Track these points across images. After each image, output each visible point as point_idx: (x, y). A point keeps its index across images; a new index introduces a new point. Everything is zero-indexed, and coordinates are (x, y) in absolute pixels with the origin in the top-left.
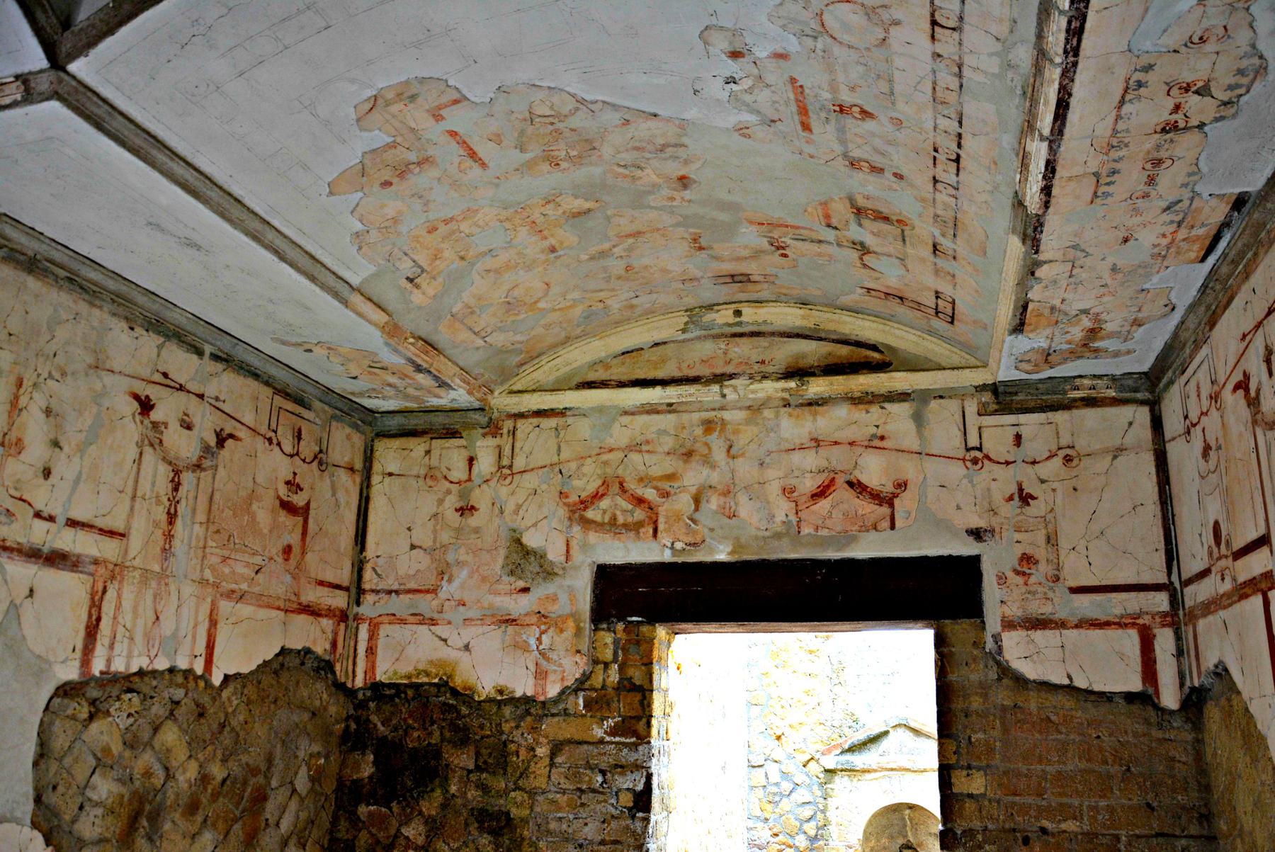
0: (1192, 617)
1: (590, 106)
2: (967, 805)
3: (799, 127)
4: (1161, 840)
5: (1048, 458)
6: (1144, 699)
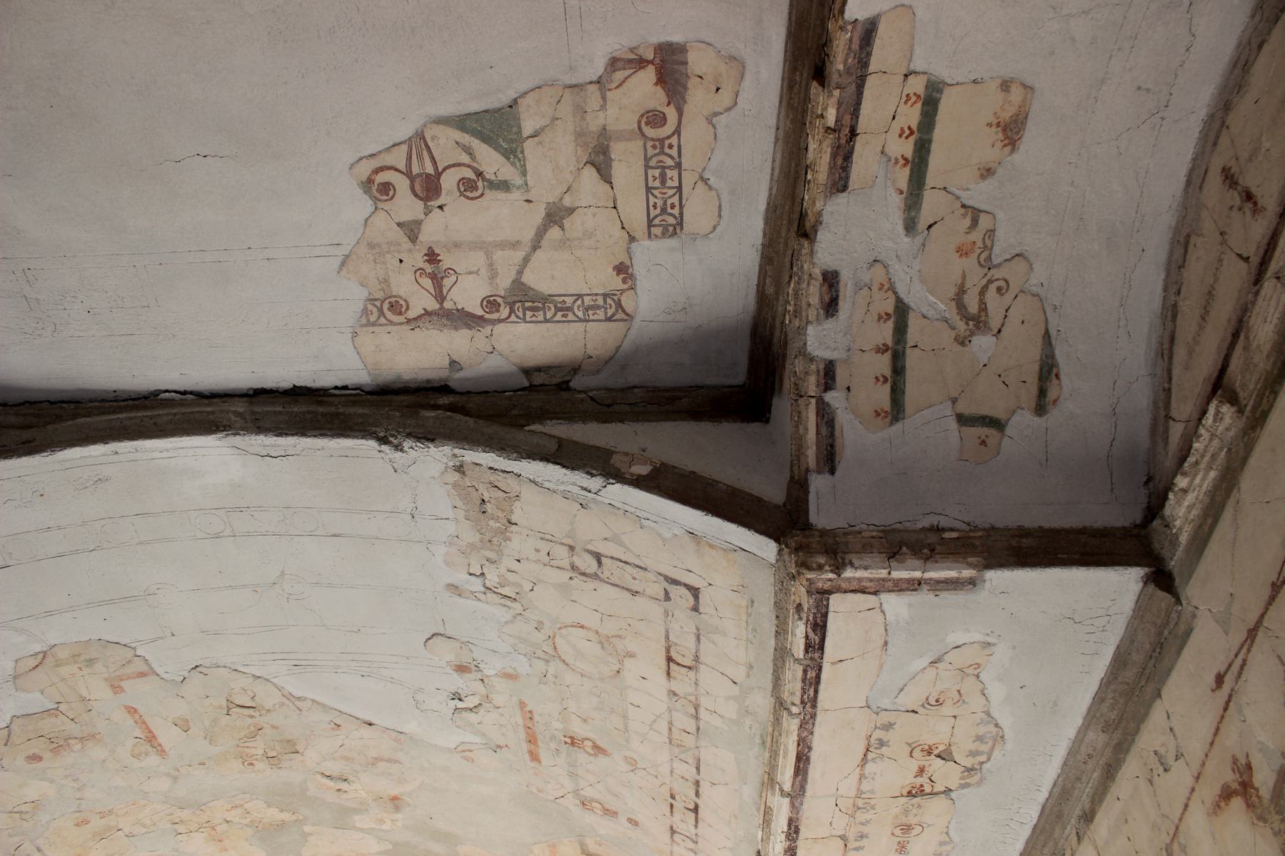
1: (296, 703)
3: (527, 757)
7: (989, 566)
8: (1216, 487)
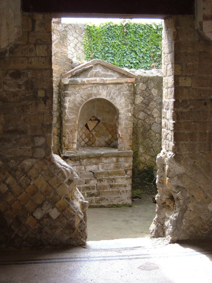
2: (184, 90)
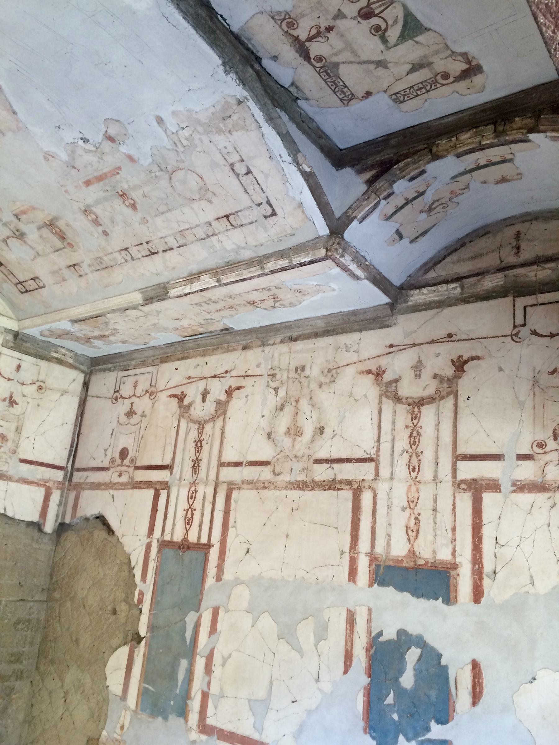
0: (79, 488)
4: (22, 603)
5: (30, 384)
6: (38, 526)
7: (367, 279)
8: (434, 302)
